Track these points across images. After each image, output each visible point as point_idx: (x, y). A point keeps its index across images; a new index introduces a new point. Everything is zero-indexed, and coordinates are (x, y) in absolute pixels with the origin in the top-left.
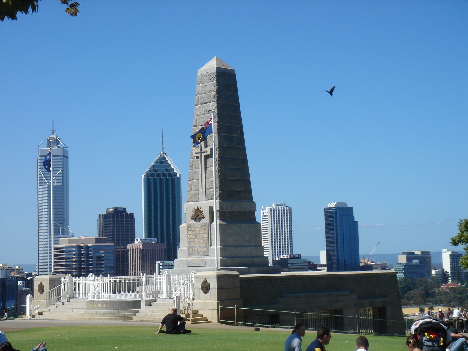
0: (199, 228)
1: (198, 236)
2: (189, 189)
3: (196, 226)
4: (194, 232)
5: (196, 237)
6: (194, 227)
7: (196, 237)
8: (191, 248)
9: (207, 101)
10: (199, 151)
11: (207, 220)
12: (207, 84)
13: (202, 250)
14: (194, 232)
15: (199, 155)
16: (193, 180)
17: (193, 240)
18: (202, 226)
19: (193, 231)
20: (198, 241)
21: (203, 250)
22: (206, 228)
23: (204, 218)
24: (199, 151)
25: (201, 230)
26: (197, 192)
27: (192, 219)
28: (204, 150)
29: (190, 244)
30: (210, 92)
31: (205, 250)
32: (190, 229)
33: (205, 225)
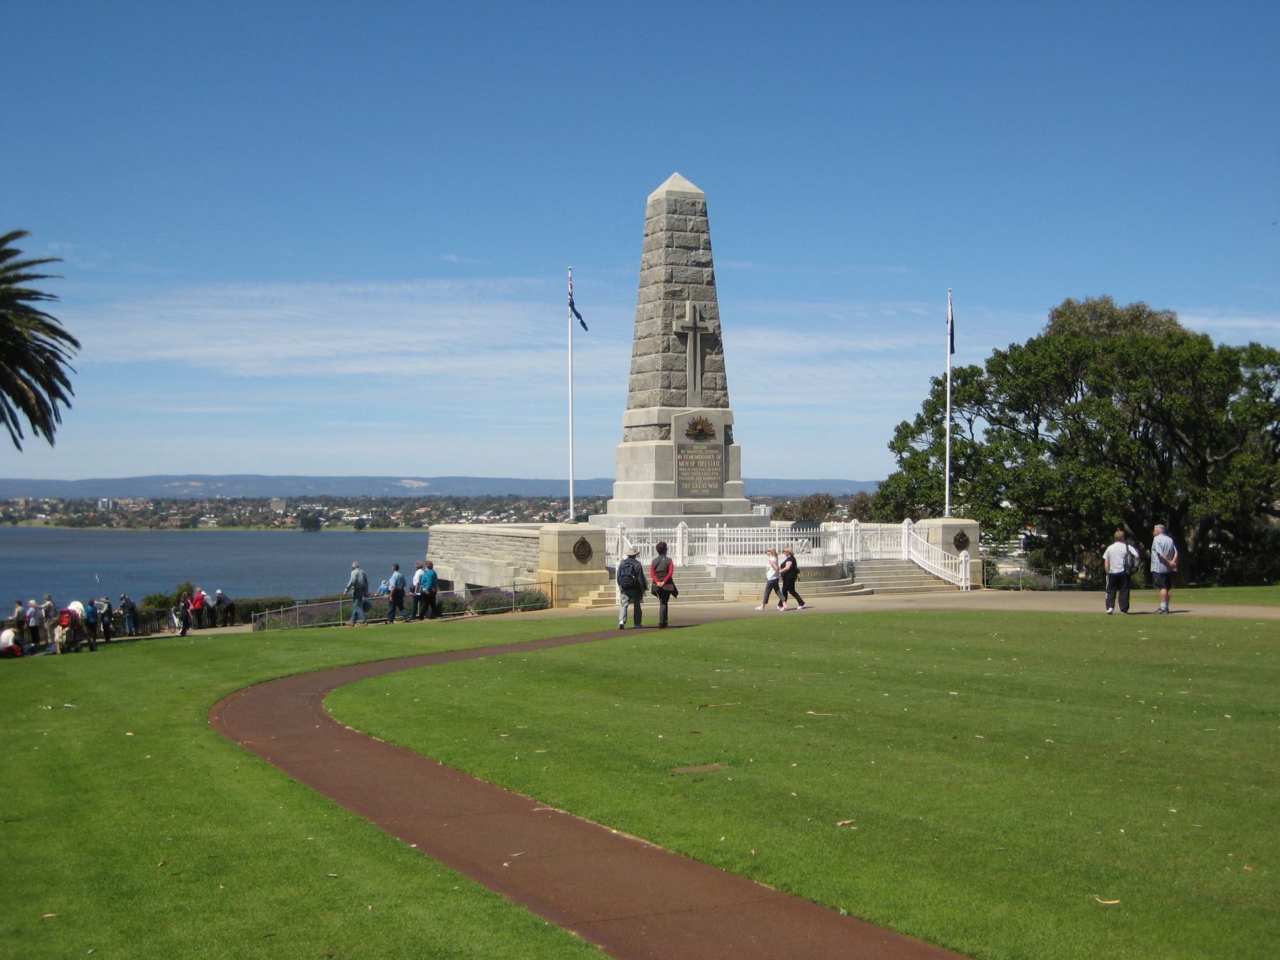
0: (704, 450)
1: (701, 464)
2: (666, 383)
3: (695, 447)
4: (692, 457)
5: (696, 465)
6: (691, 448)
7: (696, 465)
8: (685, 482)
9: (693, 245)
10: (691, 325)
11: (720, 439)
12: (690, 217)
13: (707, 486)
14: (692, 457)
15: (691, 335)
16: (671, 370)
17: (689, 469)
18: (709, 448)
19: (691, 454)
20: (701, 472)
21: (710, 486)
22: (716, 452)
23: (713, 435)
24: (691, 325)
25: (708, 454)
26: (684, 392)
27: (688, 435)
28: (700, 324)
29: (681, 476)
30: (697, 232)
31: (716, 486)
32: (682, 451)
33: (715, 447)
